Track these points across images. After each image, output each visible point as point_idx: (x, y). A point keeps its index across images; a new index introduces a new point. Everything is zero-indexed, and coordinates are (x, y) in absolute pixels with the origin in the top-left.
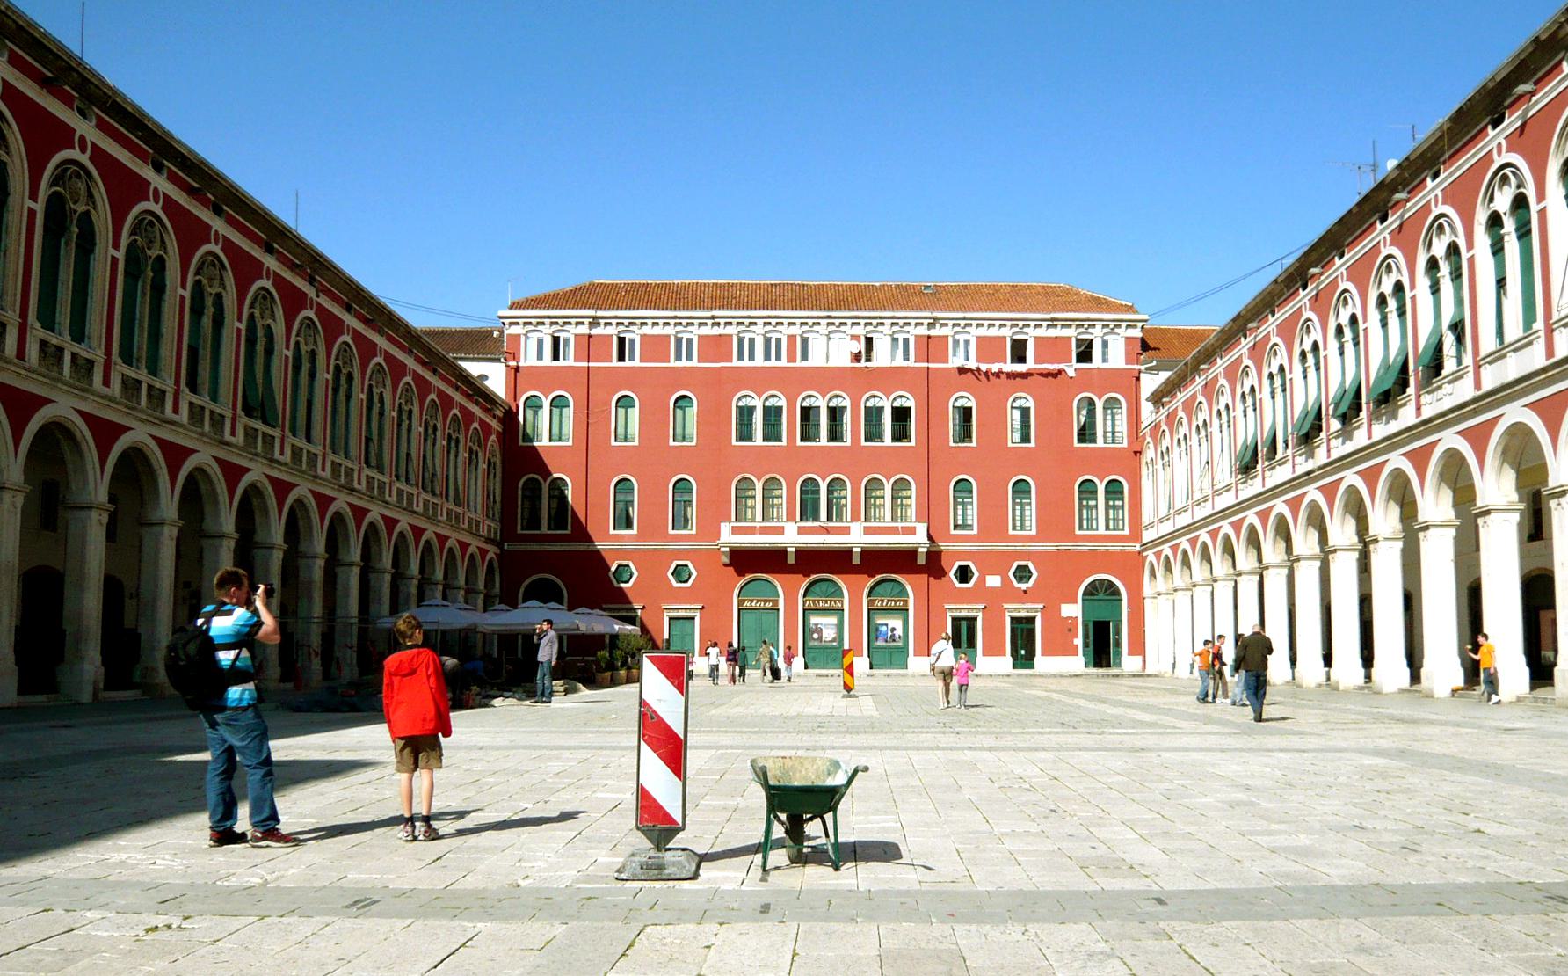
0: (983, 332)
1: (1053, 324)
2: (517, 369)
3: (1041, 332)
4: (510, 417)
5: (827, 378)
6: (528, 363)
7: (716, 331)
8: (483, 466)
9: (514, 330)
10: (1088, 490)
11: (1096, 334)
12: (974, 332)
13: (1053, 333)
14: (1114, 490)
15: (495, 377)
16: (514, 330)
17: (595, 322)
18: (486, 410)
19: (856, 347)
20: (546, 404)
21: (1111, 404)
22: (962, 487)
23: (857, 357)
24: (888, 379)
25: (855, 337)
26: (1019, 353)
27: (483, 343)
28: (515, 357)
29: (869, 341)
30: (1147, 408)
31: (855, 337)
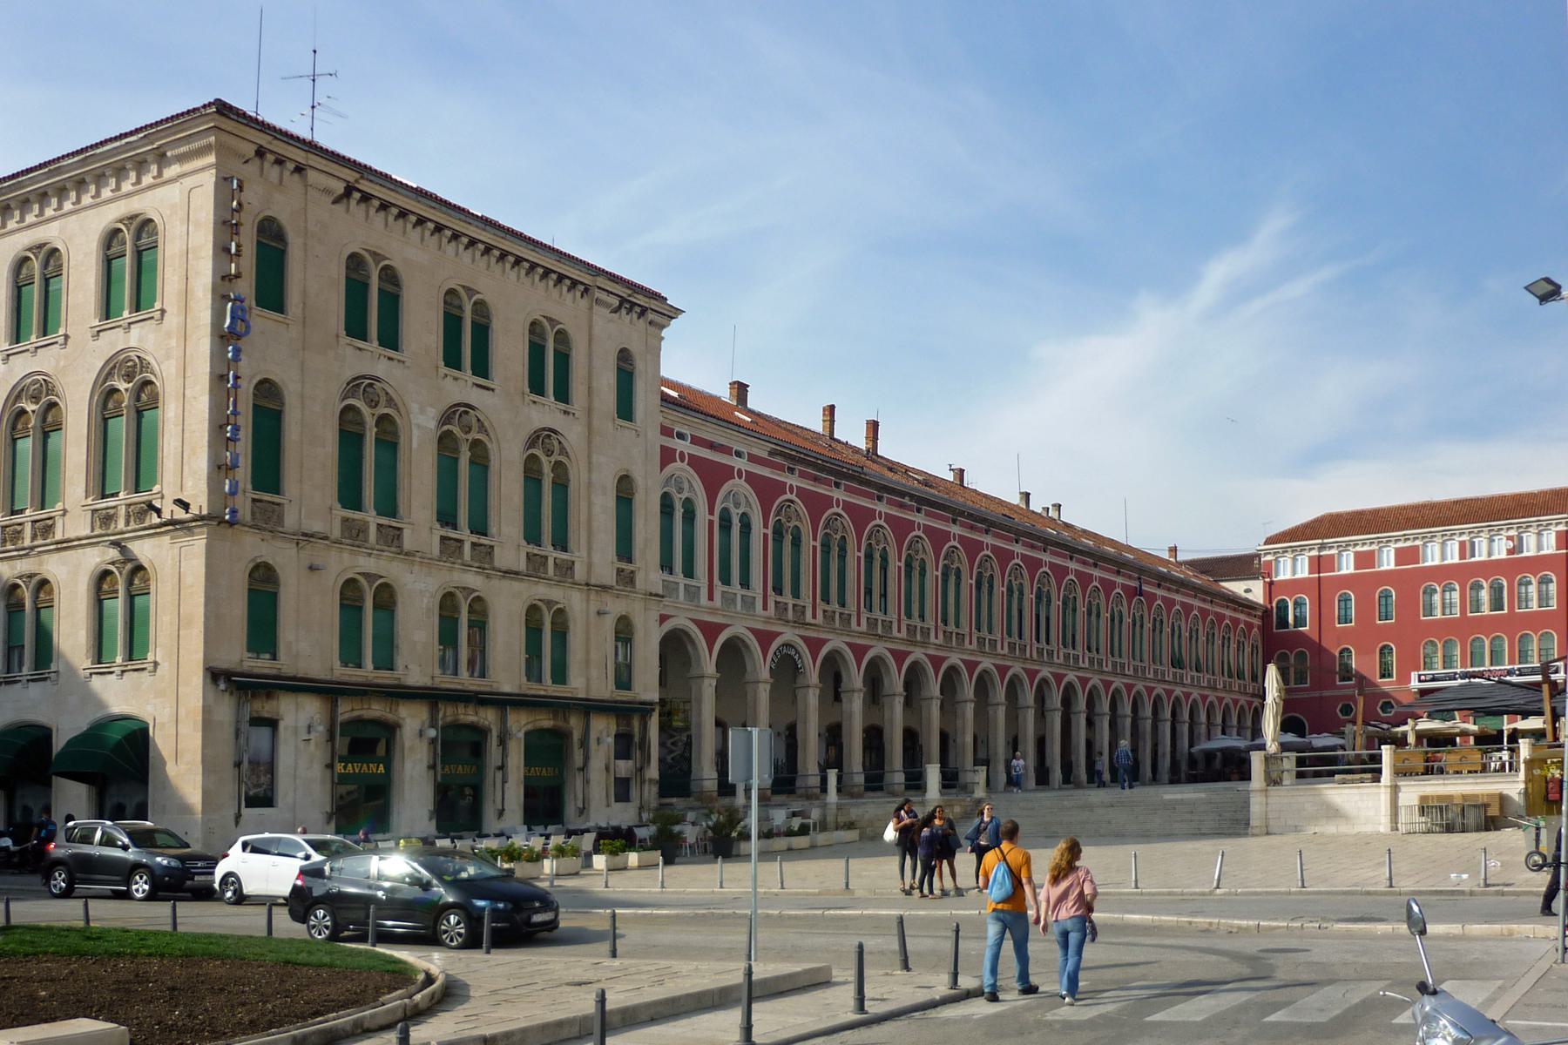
2: (1271, 583)
6: (1281, 577)
7: (1409, 544)
8: (1248, 650)
9: (1269, 558)
15: (1254, 590)
16: (1269, 558)
17: (1322, 547)
18: (1249, 614)
19: (1511, 544)
23: (1510, 552)
24: (1537, 564)
25: (1509, 538)
27: (1243, 566)
28: (1269, 575)
29: (1521, 539)
31: (1509, 538)
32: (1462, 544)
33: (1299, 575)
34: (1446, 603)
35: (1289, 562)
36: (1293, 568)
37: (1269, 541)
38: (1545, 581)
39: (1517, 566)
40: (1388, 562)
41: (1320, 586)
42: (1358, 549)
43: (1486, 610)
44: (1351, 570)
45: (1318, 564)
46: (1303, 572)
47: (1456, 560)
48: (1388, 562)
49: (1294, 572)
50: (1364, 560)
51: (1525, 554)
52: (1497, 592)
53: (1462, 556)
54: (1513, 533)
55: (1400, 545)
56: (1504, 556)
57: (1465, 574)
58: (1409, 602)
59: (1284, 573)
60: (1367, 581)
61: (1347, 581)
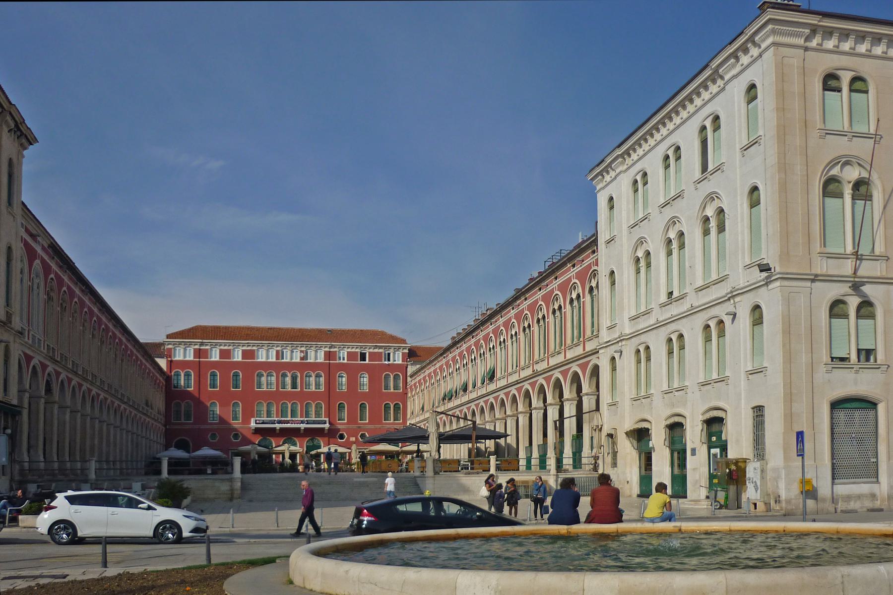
0: (349, 350)
1: (376, 347)
2: (171, 361)
3: (371, 350)
4: (168, 379)
5: (291, 366)
6: (177, 358)
7: (249, 348)
9: (170, 346)
10: (387, 407)
11: (391, 351)
12: (346, 351)
13: (376, 350)
14: (397, 407)
15: (163, 363)
16: (170, 346)
17: (202, 344)
19: (302, 355)
20: (182, 375)
21: (396, 377)
22: (341, 407)
24: (315, 366)
25: (302, 351)
26: (363, 358)
29: (307, 353)
30: (409, 379)
31: (302, 351)
32: (277, 352)
33: (187, 359)
34: (267, 382)
35: (182, 351)
36: (184, 354)
37: (168, 337)
38: (318, 376)
39: (304, 367)
40: (238, 357)
41: (200, 366)
42: (222, 347)
43: (289, 388)
44: (217, 359)
45: (199, 353)
46: (190, 357)
47: (274, 360)
48: (238, 357)
49: (185, 357)
50: (225, 354)
51: (309, 361)
52: (294, 379)
53: (277, 358)
54: (303, 349)
55: (244, 348)
56: (298, 360)
57: (278, 367)
58: (248, 379)
59: (179, 356)
60: (226, 365)
61: (215, 364)
